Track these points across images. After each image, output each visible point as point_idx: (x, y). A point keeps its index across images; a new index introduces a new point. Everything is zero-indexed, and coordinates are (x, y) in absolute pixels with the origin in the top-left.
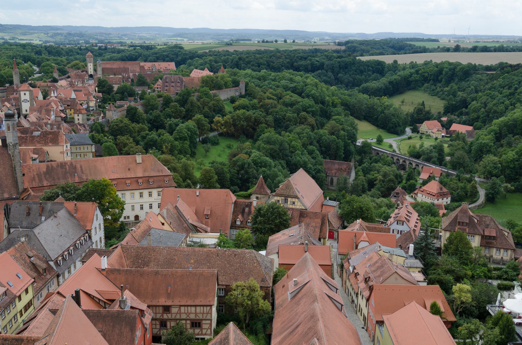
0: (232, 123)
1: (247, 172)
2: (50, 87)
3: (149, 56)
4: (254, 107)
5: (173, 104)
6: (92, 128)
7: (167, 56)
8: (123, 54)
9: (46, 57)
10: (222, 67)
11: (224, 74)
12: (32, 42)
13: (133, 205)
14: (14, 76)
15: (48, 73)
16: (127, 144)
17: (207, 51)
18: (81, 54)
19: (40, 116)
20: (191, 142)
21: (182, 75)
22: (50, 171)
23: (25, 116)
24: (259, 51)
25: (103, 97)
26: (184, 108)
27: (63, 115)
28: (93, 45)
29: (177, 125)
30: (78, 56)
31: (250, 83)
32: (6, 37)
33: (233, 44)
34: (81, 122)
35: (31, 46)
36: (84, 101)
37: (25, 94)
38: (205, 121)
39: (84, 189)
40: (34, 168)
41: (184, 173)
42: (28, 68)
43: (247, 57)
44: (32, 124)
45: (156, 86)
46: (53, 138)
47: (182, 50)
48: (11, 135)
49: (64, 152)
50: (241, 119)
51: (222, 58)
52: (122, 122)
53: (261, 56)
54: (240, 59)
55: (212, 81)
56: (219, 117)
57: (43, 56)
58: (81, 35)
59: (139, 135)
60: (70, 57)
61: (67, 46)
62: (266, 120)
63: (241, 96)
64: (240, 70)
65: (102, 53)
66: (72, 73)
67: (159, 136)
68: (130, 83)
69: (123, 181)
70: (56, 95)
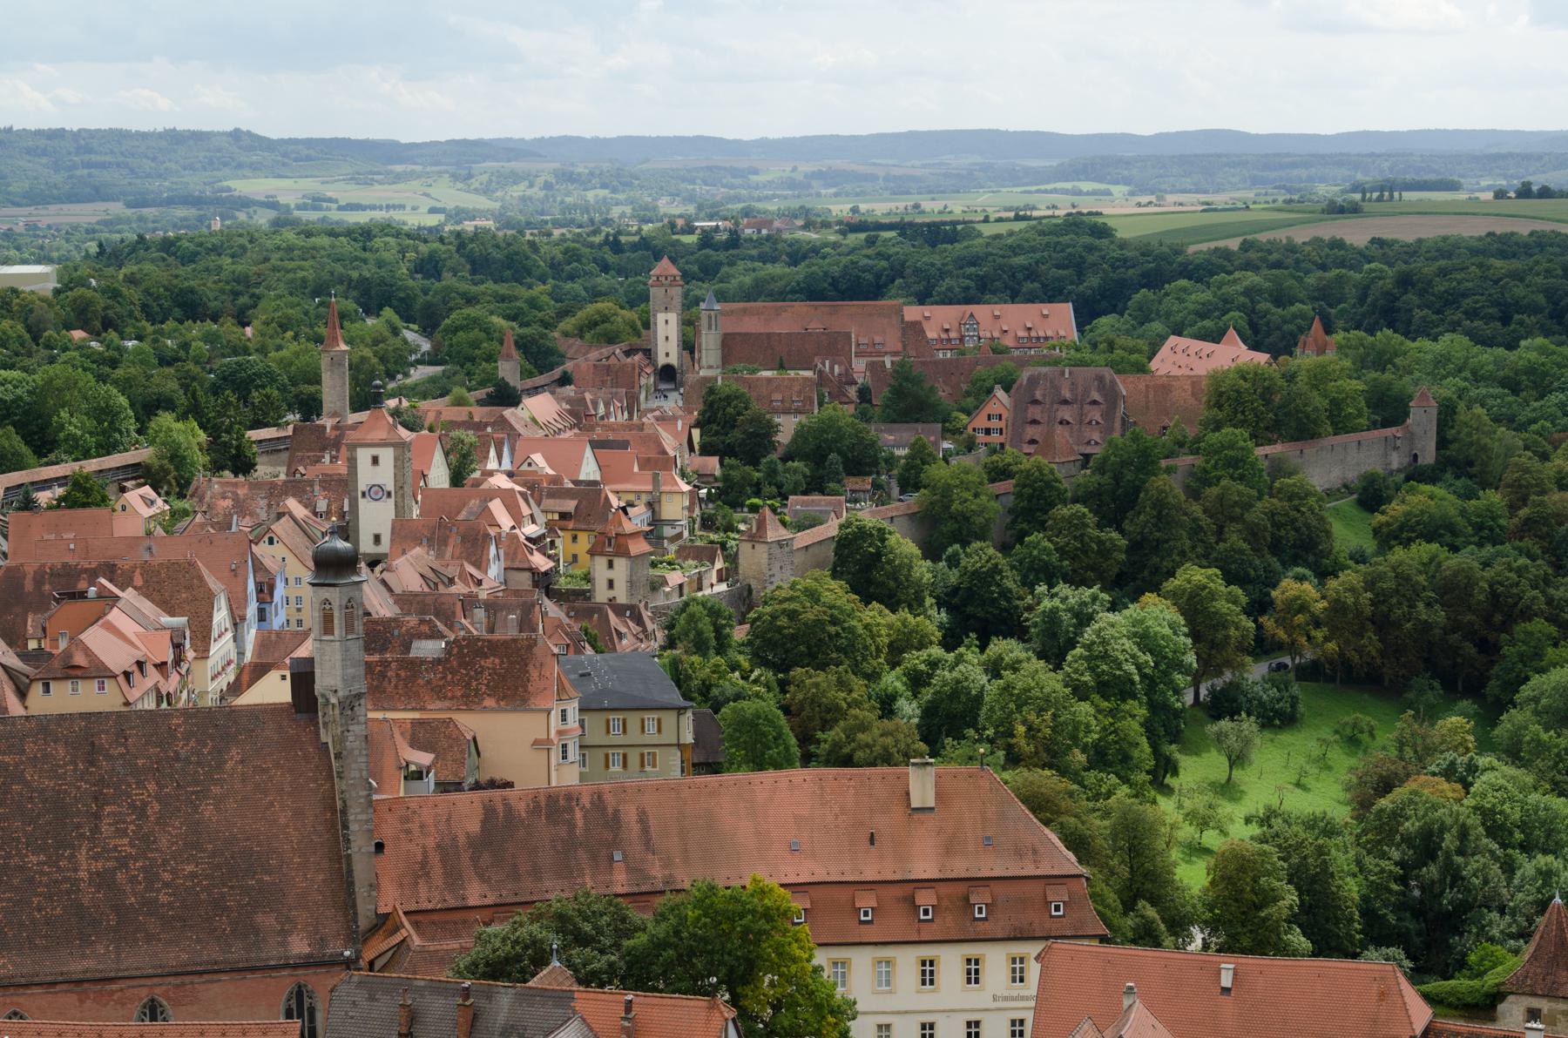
0: (1368, 610)
1: (1454, 876)
2: (479, 427)
3: (942, 274)
4: (1486, 532)
5: (1064, 511)
6: (670, 627)
7: (1031, 273)
8: (815, 266)
9: (464, 287)
10: (1317, 326)
11: (1324, 358)
12: (397, 216)
13: (884, 1020)
14: (326, 377)
15: (472, 360)
16: (838, 708)
17: (1234, 244)
18: (620, 272)
20: (1153, 706)
21: (1111, 364)
23: (373, 563)
24: (1505, 239)
25: (726, 478)
26: (1122, 532)
27: (541, 562)
28: (673, 225)
29: (1083, 618)
30: (603, 281)
31: (1461, 406)
32: (282, 200)
33: (1366, 206)
34: (622, 599)
35: (398, 234)
36: (638, 493)
37: (375, 460)
38: (1228, 601)
39: (661, 930)
41: (1124, 871)
42: (384, 340)
43: (1443, 273)
44: (405, 600)
45: (980, 421)
46: (496, 670)
47: (1105, 241)
48: (338, 657)
49: (549, 741)
50: (1417, 592)
51: (1310, 280)
52: (813, 596)
53: (1517, 264)
54: (1405, 281)
55: (1267, 394)
56: (1300, 579)
57: (448, 280)
58: (617, 180)
59: (893, 665)
60: (569, 286)
61: (557, 233)
62: (1550, 601)
63: (1417, 474)
64: (1410, 334)
65: (719, 264)
66: (581, 360)
67: (994, 669)
68: (850, 409)
69: (843, 895)
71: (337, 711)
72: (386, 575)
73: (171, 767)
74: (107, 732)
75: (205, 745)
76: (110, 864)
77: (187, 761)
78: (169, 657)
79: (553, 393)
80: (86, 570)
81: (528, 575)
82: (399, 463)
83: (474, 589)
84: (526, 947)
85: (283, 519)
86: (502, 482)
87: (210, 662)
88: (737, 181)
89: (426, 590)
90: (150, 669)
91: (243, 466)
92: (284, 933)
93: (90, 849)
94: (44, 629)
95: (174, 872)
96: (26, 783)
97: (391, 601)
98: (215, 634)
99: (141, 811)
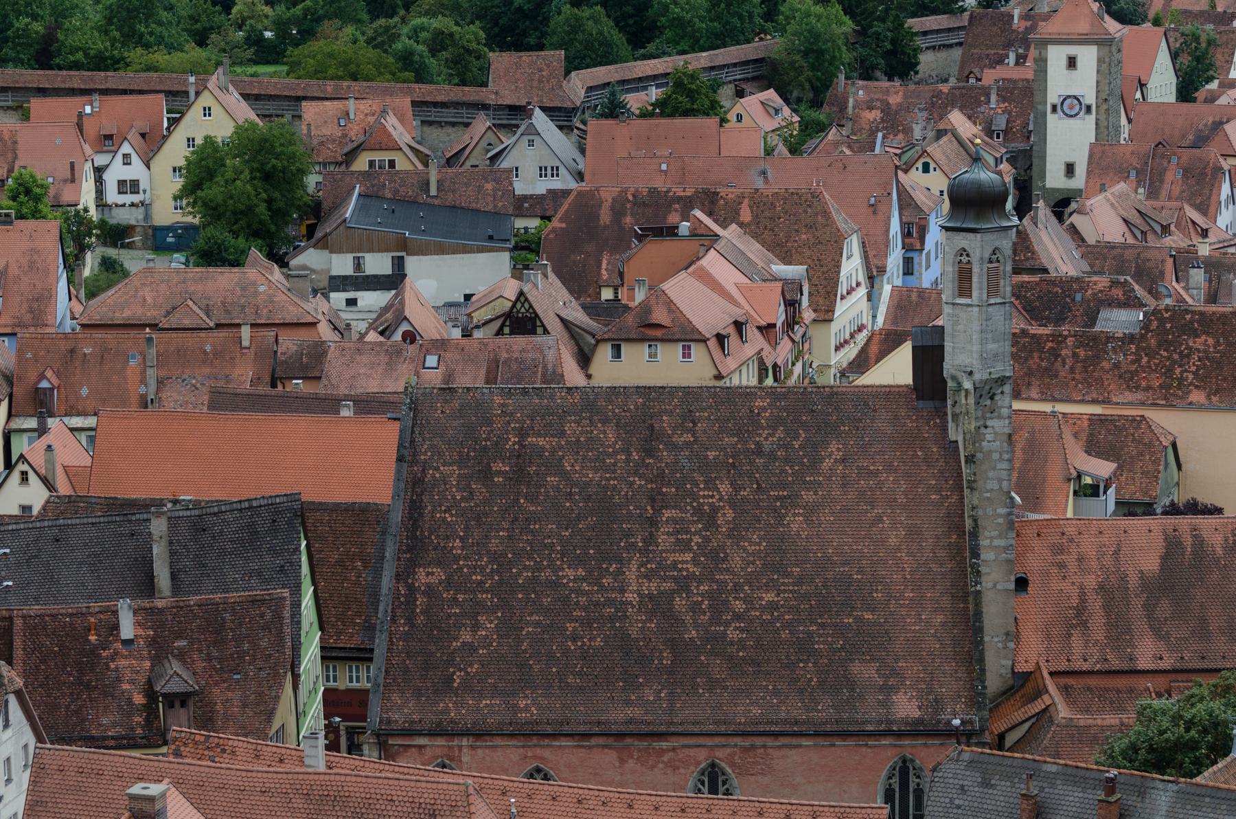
19: (1147, 206)
22: (1181, 572)
37: (1072, 63)
40: (1088, 545)
44: (1097, 254)
48: (976, 327)
71: (971, 400)
72: (1076, 219)
73: (751, 463)
74: (670, 413)
75: (797, 437)
76: (667, 586)
77: (772, 456)
78: (780, 318)
80: (679, 199)
82: (1106, 68)
83: (1196, 240)
84: (1205, 731)
85: (945, 139)
87: (835, 327)
89: (1131, 240)
90: (752, 333)
91: (900, 65)
92: (887, 690)
93: (642, 565)
94: (621, 275)
95: (748, 600)
96: (564, 475)
97: (1076, 254)
98: (842, 289)
99: (709, 519)
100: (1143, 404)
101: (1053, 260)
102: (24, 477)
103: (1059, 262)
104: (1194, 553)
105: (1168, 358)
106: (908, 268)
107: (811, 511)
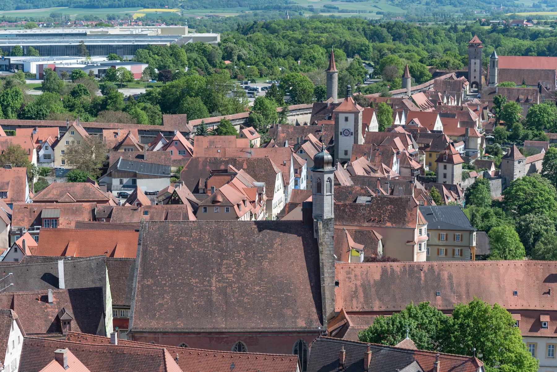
12: (363, 15)
37: (346, 119)
40: (358, 271)
70: (403, 122)
74: (225, 229)
76: (225, 284)
79: (424, 92)
81: (409, 170)
86: (399, 130)
88: (509, 3)
89: (366, 175)
90: (247, 203)
96: (192, 249)
98: (276, 190)
99: (238, 263)
100: (371, 226)
101: (342, 181)
102: (16, 250)
103: (344, 181)
104: (391, 274)
105: (380, 212)
106: (296, 184)
107: (271, 261)
